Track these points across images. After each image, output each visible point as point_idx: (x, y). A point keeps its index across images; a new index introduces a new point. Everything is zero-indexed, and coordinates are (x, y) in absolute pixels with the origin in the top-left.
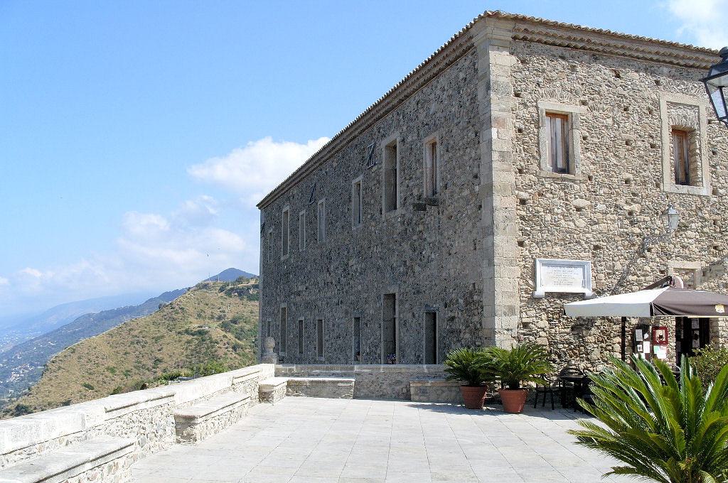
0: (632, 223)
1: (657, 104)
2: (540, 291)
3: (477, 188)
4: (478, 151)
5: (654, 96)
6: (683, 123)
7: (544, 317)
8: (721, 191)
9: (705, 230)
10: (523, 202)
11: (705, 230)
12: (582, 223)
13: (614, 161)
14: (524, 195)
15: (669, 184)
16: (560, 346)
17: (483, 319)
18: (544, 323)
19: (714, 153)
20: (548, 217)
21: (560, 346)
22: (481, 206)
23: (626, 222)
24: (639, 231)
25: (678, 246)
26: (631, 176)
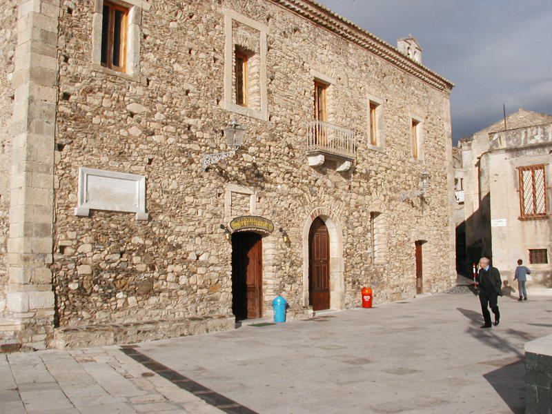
0: (192, 139)
1: (222, 16)
2: (81, 209)
3: (10, 77)
4: (15, 30)
5: (219, 10)
6: (246, 44)
7: (87, 239)
8: (278, 119)
9: (262, 155)
10: (66, 96)
11: (262, 155)
12: (135, 131)
13: (176, 67)
14: (70, 89)
15: (228, 102)
16: (106, 276)
17: (9, 240)
18: (86, 248)
19: (272, 80)
20: (96, 120)
21: (106, 276)
22: (13, 98)
23: (185, 137)
24: (198, 148)
25: (236, 169)
26: (191, 88)
